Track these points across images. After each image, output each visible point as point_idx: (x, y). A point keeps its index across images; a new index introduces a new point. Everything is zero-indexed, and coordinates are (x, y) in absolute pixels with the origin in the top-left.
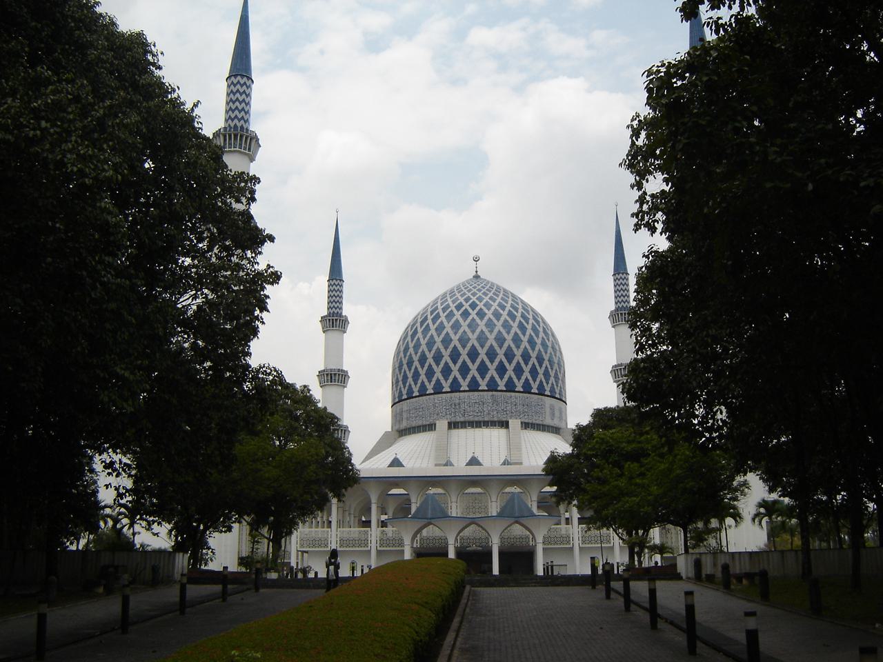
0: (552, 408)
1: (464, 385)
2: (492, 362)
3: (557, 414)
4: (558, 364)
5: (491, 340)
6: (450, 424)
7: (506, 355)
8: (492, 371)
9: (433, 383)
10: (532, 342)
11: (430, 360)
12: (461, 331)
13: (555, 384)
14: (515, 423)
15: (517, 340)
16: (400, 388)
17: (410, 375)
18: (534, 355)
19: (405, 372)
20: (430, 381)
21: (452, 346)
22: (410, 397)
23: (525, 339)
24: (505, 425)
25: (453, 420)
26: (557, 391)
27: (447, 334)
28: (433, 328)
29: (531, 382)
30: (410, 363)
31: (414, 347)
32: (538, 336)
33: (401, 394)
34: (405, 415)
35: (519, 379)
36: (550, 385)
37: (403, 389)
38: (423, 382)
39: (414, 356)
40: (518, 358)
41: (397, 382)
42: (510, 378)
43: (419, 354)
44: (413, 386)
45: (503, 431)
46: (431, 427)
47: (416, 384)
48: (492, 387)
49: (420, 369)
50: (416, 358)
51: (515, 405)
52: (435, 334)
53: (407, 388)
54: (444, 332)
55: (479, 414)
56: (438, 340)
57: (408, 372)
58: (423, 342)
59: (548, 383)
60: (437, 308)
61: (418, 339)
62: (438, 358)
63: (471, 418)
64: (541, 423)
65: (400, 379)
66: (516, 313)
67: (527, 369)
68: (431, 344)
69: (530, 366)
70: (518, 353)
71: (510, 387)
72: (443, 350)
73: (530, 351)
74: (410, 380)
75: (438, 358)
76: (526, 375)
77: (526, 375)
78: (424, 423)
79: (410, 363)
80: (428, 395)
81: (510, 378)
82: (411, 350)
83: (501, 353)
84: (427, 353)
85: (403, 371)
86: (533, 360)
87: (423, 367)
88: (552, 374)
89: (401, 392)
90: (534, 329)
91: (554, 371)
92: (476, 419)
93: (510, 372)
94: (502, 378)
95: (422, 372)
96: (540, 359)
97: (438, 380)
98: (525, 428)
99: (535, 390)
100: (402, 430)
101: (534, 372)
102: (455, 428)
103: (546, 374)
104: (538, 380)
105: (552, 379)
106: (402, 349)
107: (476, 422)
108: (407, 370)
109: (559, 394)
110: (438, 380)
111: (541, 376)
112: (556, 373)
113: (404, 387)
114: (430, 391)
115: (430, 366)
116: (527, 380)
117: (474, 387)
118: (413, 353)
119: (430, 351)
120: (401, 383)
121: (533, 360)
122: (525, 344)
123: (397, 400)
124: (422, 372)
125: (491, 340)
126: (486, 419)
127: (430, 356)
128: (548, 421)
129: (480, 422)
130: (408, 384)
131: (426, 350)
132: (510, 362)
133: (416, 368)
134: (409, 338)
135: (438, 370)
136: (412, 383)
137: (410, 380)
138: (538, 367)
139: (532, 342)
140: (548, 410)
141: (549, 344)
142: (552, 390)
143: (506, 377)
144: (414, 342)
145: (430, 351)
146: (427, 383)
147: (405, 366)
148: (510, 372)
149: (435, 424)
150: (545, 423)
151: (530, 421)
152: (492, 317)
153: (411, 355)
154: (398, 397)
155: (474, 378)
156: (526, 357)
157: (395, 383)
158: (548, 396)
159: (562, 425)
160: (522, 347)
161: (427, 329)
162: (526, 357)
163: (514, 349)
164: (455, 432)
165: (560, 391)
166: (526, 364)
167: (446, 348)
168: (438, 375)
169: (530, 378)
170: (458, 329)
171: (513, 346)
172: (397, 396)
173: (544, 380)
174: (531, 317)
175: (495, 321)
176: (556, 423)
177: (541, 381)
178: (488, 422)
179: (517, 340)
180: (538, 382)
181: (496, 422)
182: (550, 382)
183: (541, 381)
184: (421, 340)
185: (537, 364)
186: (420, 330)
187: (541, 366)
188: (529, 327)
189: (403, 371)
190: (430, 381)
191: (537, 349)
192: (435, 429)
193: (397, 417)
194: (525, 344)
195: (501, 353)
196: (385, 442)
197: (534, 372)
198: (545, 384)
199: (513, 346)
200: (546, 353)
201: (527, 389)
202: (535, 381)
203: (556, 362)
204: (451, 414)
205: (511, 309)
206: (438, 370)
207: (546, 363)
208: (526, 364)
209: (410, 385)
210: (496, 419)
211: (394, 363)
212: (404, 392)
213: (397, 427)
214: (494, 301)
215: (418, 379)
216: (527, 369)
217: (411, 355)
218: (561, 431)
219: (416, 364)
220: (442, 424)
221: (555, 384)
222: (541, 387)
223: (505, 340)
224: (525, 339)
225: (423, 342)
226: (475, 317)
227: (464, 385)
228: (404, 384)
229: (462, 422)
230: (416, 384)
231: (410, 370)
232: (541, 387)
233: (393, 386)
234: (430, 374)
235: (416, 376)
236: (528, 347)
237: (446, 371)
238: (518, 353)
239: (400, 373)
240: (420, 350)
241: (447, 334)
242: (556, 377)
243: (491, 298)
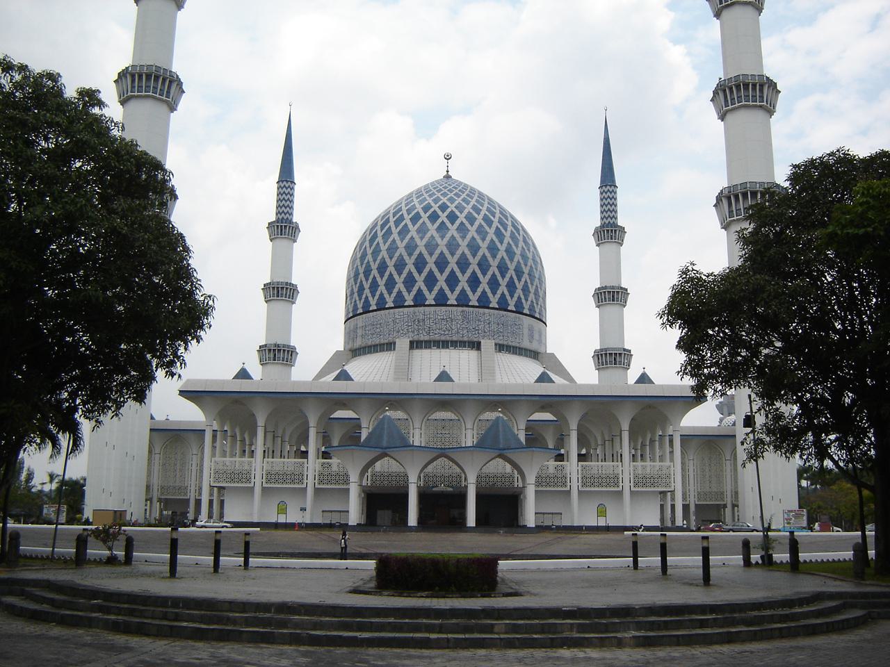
0: (531, 330)
1: (430, 298)
2: (463, 272)
3: (536, 336)
4: (539, 279)
5: (463, 247)
6: (412, 343)
7: (479, 265)
8: (463, 284)
9: (394, 295)
10: (509, 252)
12: (428, 235)
13: (535, 301)
14: (488, 345)
15: (493, 249)
16: (355, 301)
17: (367, 286)
18: (512, 266)
19: (361, 281)
20: (390, 293)
21: (417, 252)
22: (366, 312)
23: (502, 248)
24: (476, 346)
25: (416, 338)
26: (537, 311)
27: (412, 238)
28: (395, 231)
29: (508, 297)
30: (367, 272)
31: (373, 253)
32: (517, 246)
33: (355, 308)
34: (360, 332)
35: (494, 293)
36: (529, 303)
37: (358, 302)
38: (382, 294)
39: (372, 264)
40: (493, 269)
41: (352, 293)
42: (484, 292)
43: (378, 262)
44: (370, 299)
45: (473, 354)
46: (390, 346)
47: (373, 296)
48: (463, 301)
49: (378, 279)
50: (374, 266)
51: (489, 323)
52: (397, 238)
53: (363, 300)
54: (409, 237)
55: (447, 332)
56: (401, 245)
57: (364, 283)
58: (384, 248)
59: (527, 300)
60: (400, 209)
61: (378, 244)
62: (400, 266)
63: (437, 337)
64: (518, 345)
65: (356, 290)
66: (492, 218)
67: (503, 283)
68: (392, 249)
69: (507, 279)
70: (494, 263)
71: (484, 303)
72: (406, 257)
73: (508, 262)
74: (367, 292)
75: (400, 266)
76: (503, 289)
77: (503, 289)
78: (382, 342)
79: (367, 272)
81: (484, 292)
82: (369, 257)
83: (474, 262)
84: (388, 260)
85: (359, 281)
86: (511, 273)
87: (382, 277)
88: (532, 290)
89: (355, 305)
90: (513, 237)
91: (534, 287)
92: (443, 338)
93: (484, 286)
95: (382, 283)
96: (519, 272)
97: (400, 292)
98: (500, 351)
99: (511, 307)
100: (356, 350)
101: (511, 286)
102: (417, 348)
103: (526, 290)
104: (516, 296)
105: (531, 297)
106: (359, 256)
107: (443, 342)
108: (364, 279)
109: (540, 314)
110: (400, 292)
111: (519, 292)
112: (536, 290)
113: (360, 299)
116: (503, 294)
117: (441, 301)
118: (371, 260)
119: (391, 258)
120: (356, 295)
121: (511, 273)
122: (502, 253)
123: (351, 315)
124: (382, 283)
125: (463, 247)
126: (455, 338)
127: (391, 264)
128: (526, 344)
129: (447, 342)
130: (364, 296)
131: (386, 256)
132: (484, 274)
133: (374, 278)
134: (367, 244)
135: (399, 280)
136: (369, 295)
137: (367, 292)
138: (516, 281)
139: (509, 252)
140: (526, 331)
141: (530, 256)
142: (532, 308)
143: (480, 290)
144: (373, 248)
145: (391, 258)
146: (386, 296)
147: (362, 276)
148: (484, 286)
149: (395, 343)
150: (522, 346)
151: (505, 343)
152: (465, 221)
153: (368, 262)
154: (353, 311)
156: (503, 269)
157: (350, 295)
158: (526, 315)
159: (541, 350)
160: (499, 257)
161: (389, 232)
162: (503, 269)
163: (490, 259)
164: (418, 353)
165: (541, 310)
166: (503, 277)
167: (410, 255)
168: (400, 286)
169: (506, 293)
170: (425, 234)
171: (488, 255)
172: (351, 310)
176: (534, 346)
177: (519, 298)
178: (456, 342)
179: (493, 249)
180: (515, 299)
181: (465, 342)
182: (530, 299)
183: (519, 298)
184: (381, 245)
185: (515, 277)
186: (380, 234)
187: (519, 280)
188: (508, 234)
189: (359, 281)
190: (390, 293)
191: (516, 260)
192: (394, 349)
193: (350, 335)
194: (502, 253)
195: (474, 262)
196: (338, 362)
197: (511, 286)
198: (523, 301)
199: (488, 255)
200: (526, 265)
201: (503, 306)
202: (512, 296)
203: (537, 276)
204: (413, 332)
205: (487, 213)
206: (399, 280)
207: (525, 277)
208: (503, 277)
209: (367, 297)
210: (465, 339)
211: (349, 272)
212: (360, 305)
213: (349, 347)
216: (503, 283)
217: (368, 262)
218: (540, 356)
219: (375, 272)
220: (403, 343)
221: (535, 301)
222: (519, 304)
224: (502, 248)
225: (384, 248)
227: (430, 298)
228: (360, 296)
229: (426, 342)
230: (373, 296)
231: (367, 280)
232: (519, 304)
233: (346, 299)
234: (390, 284)
235: (374, 286)
236: (506, 257)
237: (409, 282)
238: (494, 263)
239: (356, 284)
240: (380, 258)
241: (412, 238)
242: (536, 293)
243: (464, 200)
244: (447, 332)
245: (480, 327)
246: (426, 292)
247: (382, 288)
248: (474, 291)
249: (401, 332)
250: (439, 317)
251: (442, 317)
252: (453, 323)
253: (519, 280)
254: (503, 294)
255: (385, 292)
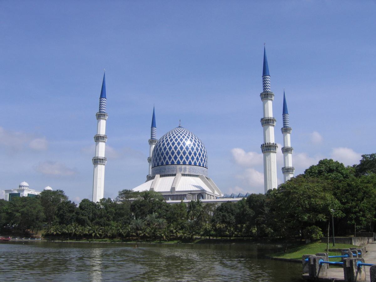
8: (184, 159)
11: (165, 154)
17: (158, 159)
20: (165, 161)
21: (172, 150)
23: (195, 148)
26: (205, 165)
28: (166, 144)
29: (197, 162)
30: (158, 155)
42: (190, 161)
47: (160, 162)
65: (155, 160)
67: (195, 158)
69: (196, 157)
70: (193, 153)
76: (195, 160)
77: (195, 160)
83: (187, 152)
84: (164, 152)
86: (197, 155)
93: (190, 159)
99: (198, 165)
113: (156, 162)
116: (195, 161)
120: (155, 161)
121: (197, 155)
122: (195, 150)
123: (154, 166)
131: (163, 151)
137: (158, 160)
143: (189, 160)
146: (164, 162)
147: (157, 156)
148: (190, 159)
155: (178, 160)
156: (195, 154)
160: (194, 151)
168: (167, 159)
172: (153, 165)
173: (201, 162)
174: (197, 141)
177: (200, 162)
187: (200, 157)
195: (187, 152)
202: (198, 162)
208: (195, 156)
212: (156, 164)
216: (195, 158)
223: (189, 148)
224: (195, 148)
230: (160, 162)
232: (203, 164)
246: (174, 161)
247: (162, 160)
248: (187, 160)
253: (200, 157)
254: (195, 161)
255: (163, 160)
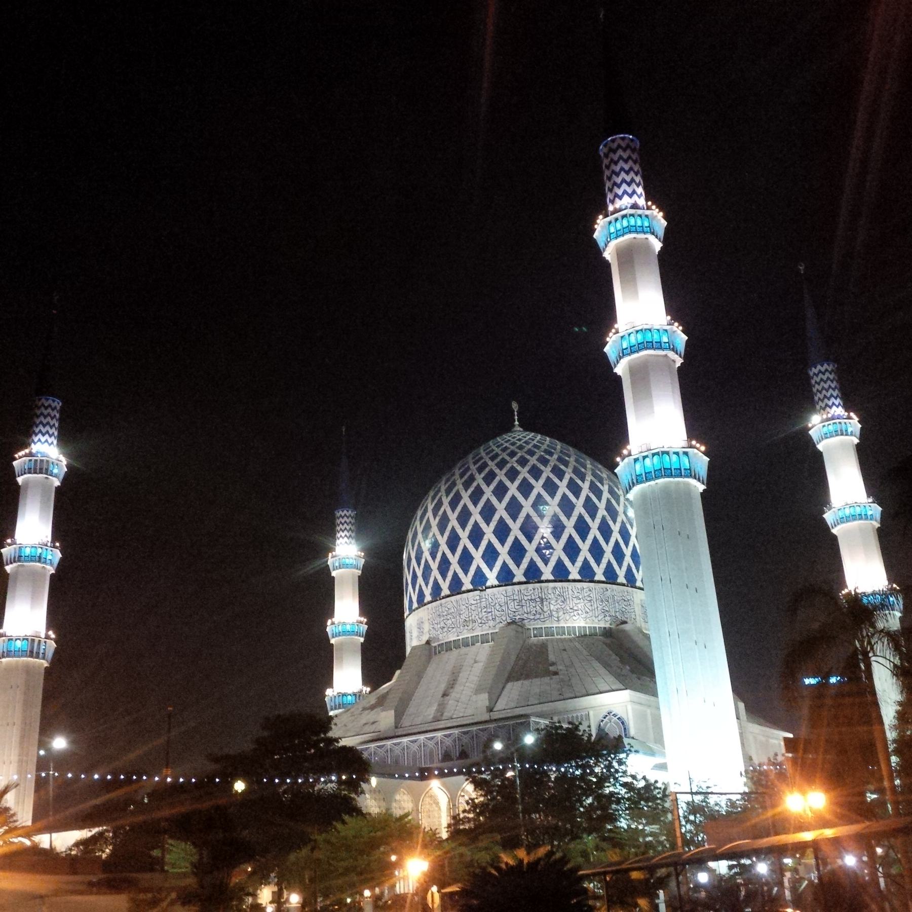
20: (466, 572)
38: (455, 574)
51: (590, 601)
55: (538, 616)
66: (583, 470)
80: (464, 592)
94: (573, 562)
95: (454, 560)
114: (467, 585)
115: (465, 549)
124: (454, 560)
175: (556, 480)
214: (551, 454)
215: (448, 569)
226: (528, 476)
243: (546, 451)
244: (538, 616)
245: (579, 606)
247: (455, 567)
249: (479, 621)
250: (526, 598)
251: (529, 598)
252: (545, 603)
